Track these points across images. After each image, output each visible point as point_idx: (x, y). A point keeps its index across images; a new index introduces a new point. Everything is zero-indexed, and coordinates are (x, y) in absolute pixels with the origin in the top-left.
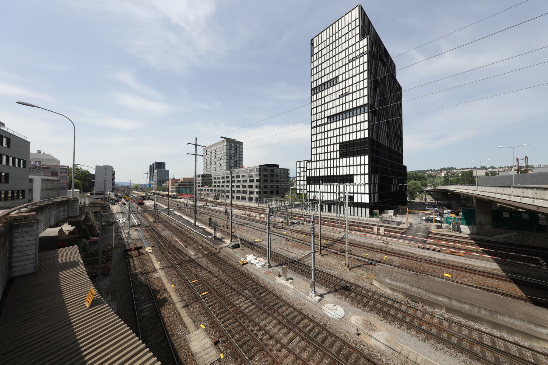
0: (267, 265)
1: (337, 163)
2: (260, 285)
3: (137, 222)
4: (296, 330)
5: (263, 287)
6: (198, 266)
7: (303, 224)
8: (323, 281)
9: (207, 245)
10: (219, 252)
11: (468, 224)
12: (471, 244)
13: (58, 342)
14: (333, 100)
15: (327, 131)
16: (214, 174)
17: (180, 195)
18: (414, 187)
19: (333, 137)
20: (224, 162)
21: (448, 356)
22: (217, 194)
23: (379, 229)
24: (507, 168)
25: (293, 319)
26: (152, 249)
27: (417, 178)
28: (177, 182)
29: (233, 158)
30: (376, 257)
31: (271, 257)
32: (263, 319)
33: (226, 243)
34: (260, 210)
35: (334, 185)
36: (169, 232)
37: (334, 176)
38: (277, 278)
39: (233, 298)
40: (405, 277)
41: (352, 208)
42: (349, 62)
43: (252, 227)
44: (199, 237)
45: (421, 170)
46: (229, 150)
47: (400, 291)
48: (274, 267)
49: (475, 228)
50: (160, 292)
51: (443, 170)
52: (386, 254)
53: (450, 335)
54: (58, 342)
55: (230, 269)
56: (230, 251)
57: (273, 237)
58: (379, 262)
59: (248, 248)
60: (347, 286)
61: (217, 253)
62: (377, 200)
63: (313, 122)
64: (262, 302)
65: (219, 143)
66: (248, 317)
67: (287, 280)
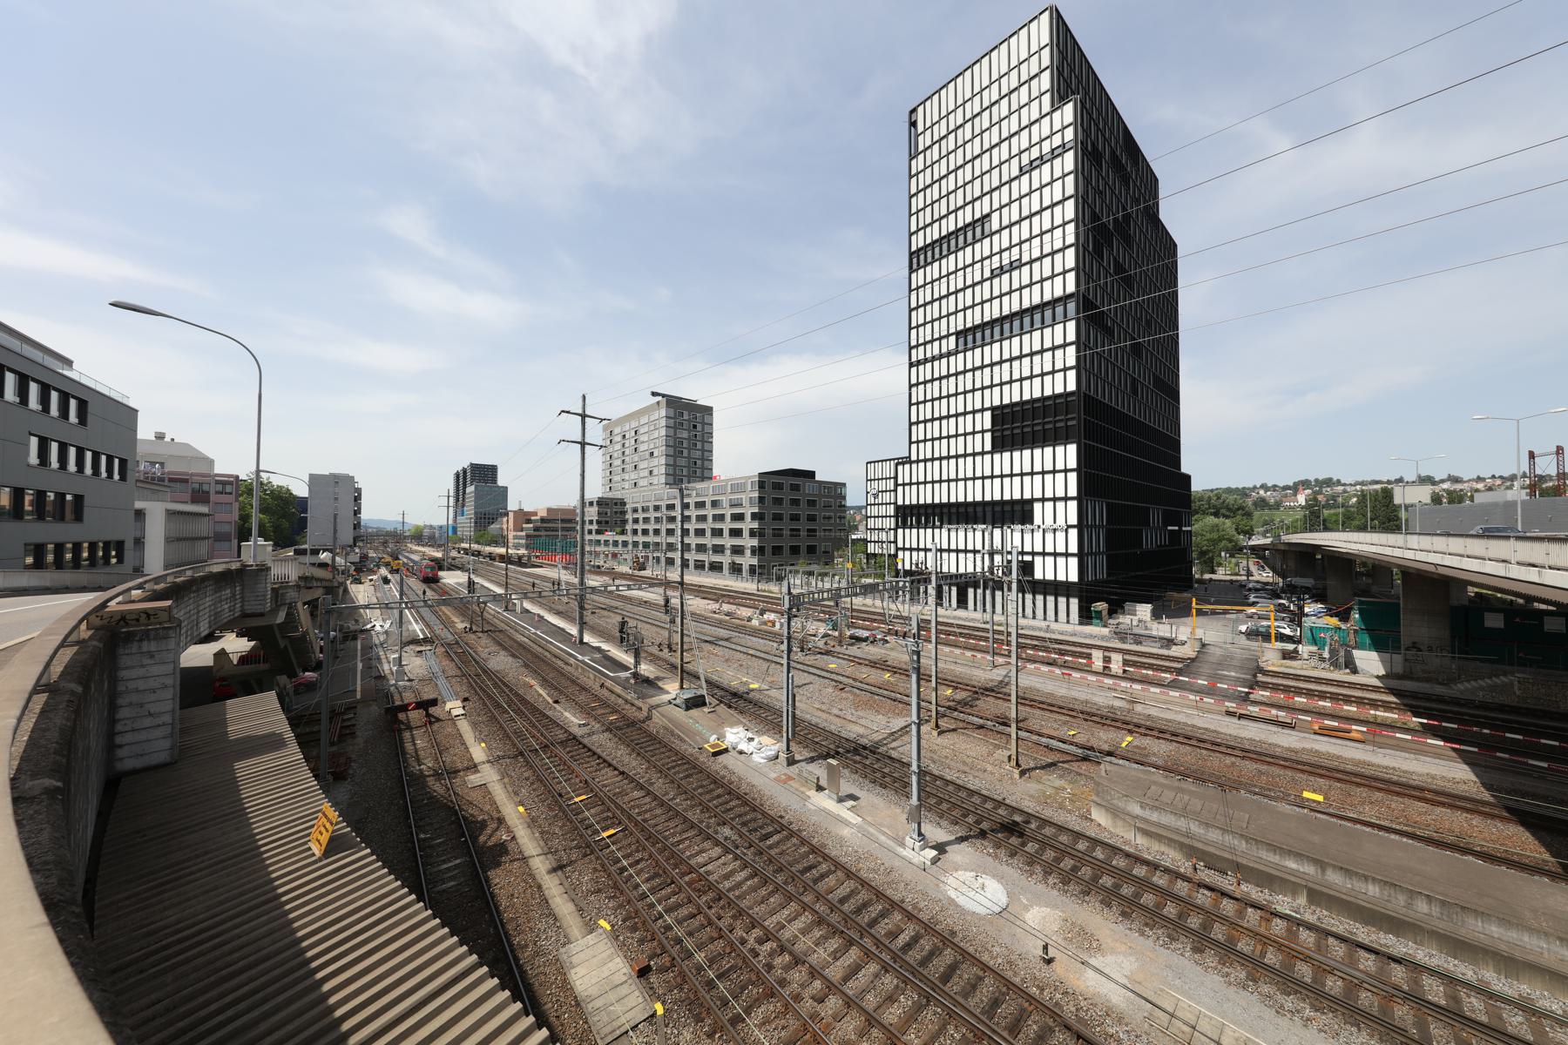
0: (783, 756)
1: (984, 465)
2: (764, 814)
3: (422, 630)
4: (868, 942)
5: (773, 820)
6: (589, 757)
7: (887, 642)
8: (945, 806)
9: (613, 698)
10: (649, 718)
11: (1378, 645)
12: (1386, 706)
13: (248, 944)
14: (974, 285)
15: (957, 374)
16: (633, 499)
17: (537, 557)
18: (1214, 535)
19: (973, 390)
20: (660, 464)
21: (1316, 1031)
22: (640, 555)
23: (1107, 660)
24: (1498, 482)
25: (858, 911)
26: (464, 707)
27: (1223, 511)
28: (529, 521)
29: (685, 453)
30: (1100, 739)
31: (794, 733)
32: (774, 909)
33: (668, 693)
34: (763, 602)
35: (974, 530)
36: (510, 659)
37: (975, 504)
38: (812, 793)
39: (690, 846)
40: (1186, 798)
41: (1029, 597)
42: (1022, 172)
43: (739, 648)
44: (591, 676)
45: (1234, 487)
46: (675, 428)
47: (1170, 840)
48: (803, 764)
49: (1398, 658)
50: (487, 826)
51: (1301, 487)
52: (1130, 732)
53: (1322, 970)
54: (248, 944)
55: (679, 765)
56: (679, 714)
57: (799, 678)
58: (1110, 754)
59: (730, 707)
60: (1014, 821)
61: (644, 722)
62: (1103, 575)
63: (914, 347)
64: (771, 861)
66: (730, 903)
67: (841, 800)
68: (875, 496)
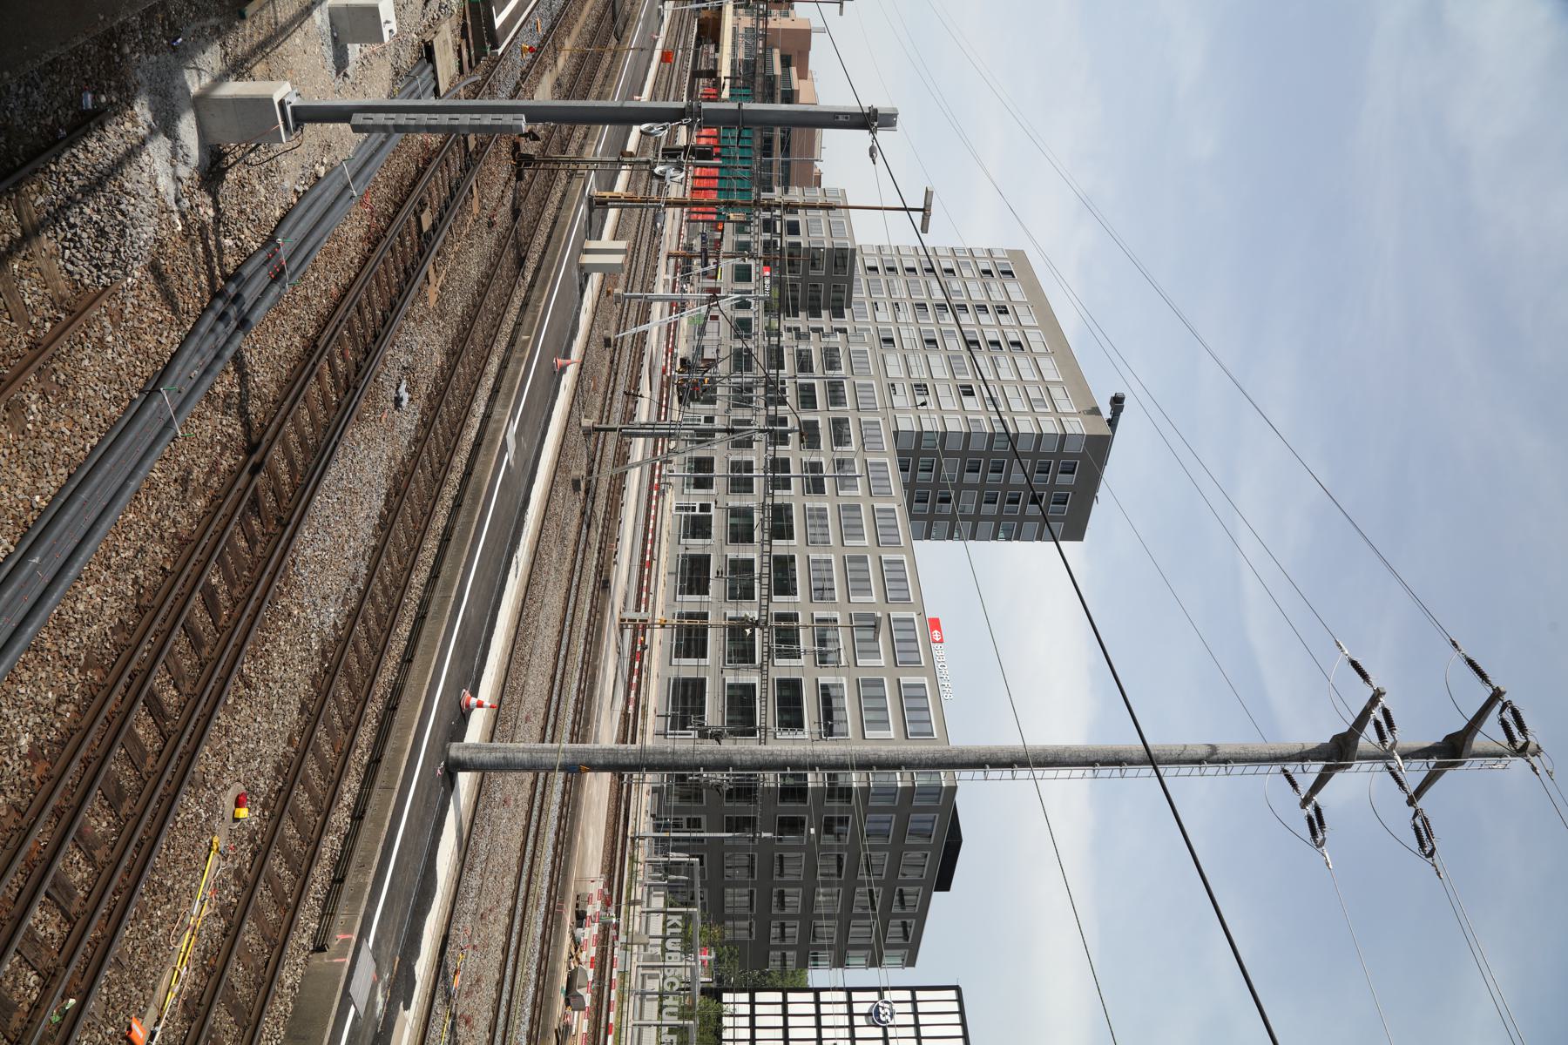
28: (786, 62)
29: (970, 478)
65: (1075, 379)
68: (874, 1017)
